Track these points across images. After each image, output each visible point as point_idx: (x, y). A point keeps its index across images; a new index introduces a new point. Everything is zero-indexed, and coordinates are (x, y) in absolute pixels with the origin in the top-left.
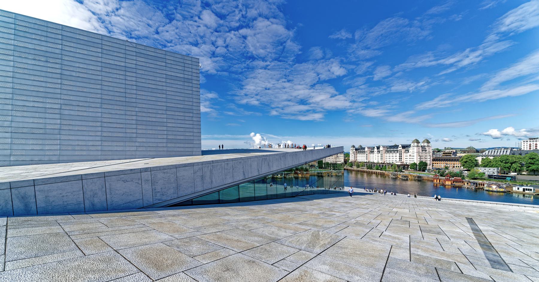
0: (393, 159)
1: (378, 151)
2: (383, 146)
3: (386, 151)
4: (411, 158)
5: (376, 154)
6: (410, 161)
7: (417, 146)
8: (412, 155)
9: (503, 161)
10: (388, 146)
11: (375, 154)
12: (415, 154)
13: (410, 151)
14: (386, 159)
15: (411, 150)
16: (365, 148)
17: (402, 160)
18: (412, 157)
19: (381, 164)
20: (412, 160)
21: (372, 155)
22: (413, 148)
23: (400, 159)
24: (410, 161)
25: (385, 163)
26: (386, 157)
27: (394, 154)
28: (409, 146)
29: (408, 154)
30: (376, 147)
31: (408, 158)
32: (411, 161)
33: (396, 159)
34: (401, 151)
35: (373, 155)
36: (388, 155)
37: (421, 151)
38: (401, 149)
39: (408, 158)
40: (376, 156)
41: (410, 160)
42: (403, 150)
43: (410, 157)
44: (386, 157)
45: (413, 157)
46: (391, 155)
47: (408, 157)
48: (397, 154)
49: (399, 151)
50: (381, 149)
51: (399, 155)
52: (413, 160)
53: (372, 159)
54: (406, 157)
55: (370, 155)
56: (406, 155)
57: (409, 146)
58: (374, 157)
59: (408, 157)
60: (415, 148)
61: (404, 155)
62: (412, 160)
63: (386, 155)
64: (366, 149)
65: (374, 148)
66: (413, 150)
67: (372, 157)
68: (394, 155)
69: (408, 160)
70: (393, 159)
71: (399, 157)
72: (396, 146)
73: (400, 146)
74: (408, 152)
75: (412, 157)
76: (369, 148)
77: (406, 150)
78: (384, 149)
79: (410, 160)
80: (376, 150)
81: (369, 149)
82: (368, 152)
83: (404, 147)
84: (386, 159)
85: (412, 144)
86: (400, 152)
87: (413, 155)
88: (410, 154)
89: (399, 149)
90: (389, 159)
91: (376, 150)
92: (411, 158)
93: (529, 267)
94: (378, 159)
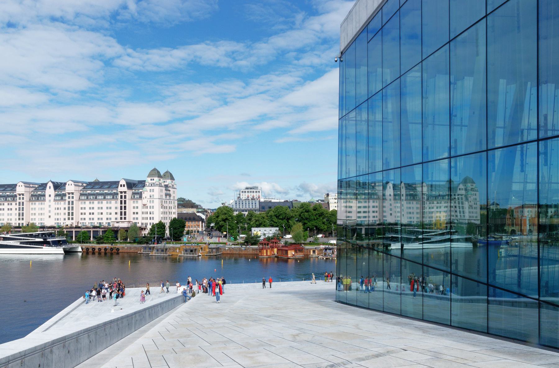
0: (100, 216)
1: (56, 195)
2: (75, 182)
3: (81, 195)
4: (147, 213)
5: (53, 203)
6: (143, 218)
7: (160, 185)
8: (149, 205)
9: (279, 216)
10: (85, 183)
11: (47, 203)
12: (157, 203)
13: (143, 196)
14: (83, 216)
15: (146, 192)
16: (16, 185)
17: (127, 216)
18: (148, 210)
19: (92, 230)
20: (149, 216)
21: (37, 205)
22: (152, 188)
23: (123, 214)
24: (143, 218)
25: (80, 225)
26: (83, 211)
27: (105, 202)
28: (142, 184)
29: (140, 203)
30: (50, 184)
31: (140, 213)
32: (147, 218)
33: (109, 216)
34: (123, 194)
35: (42, 206)
36: (87, 204)
37: (164, 197)
38: (125, 189)
39: (140, 213)
40: (52, 209)
41: (145, 216)
42: (129, 193)
43: (145, 210)
44: (83, 211)
45: (152, 210)
46: (96, 204)
47: (140, 210)
48: (113, 202)
49: (120, 195)
50: (70, 188)
51: (119, 205)
52: (152, 216)
53: (37, 217)
54: (136, 210)
55: (33, 206)
56: (136, 205)
57: (142, 184)
58: (46, 211)
59: (140, 210)
60: (157, 189)
61: (130, 204)
62: (149, 216)
63: (83, 206)
64: (20, 189)
65: (43, 186)
66: (152, 193)
67: (37, 212)
68: (105, 204)
69: (140, 216)
70: (100, 216)
71: (119, 211)
72: (115, 184)
73: (123, 182)
74: (141, 197)
75: (148, 210)
76: (27, 185)
77: (133, 193)
78: (77, 188)
79: (145, 216)
80: (50, 191)
81: (28, 189)
82: (27, 197)
83: (131, 185)
84: (83, 216)
85: (148, 180)
86: (121, 197)
87: (152, 205)
88: (145, 201)
89: (120, 189)
90: (92, 216)
91: (50, 191)
92: (147, 213)
93: (500, 359)
94: (57, 217)
